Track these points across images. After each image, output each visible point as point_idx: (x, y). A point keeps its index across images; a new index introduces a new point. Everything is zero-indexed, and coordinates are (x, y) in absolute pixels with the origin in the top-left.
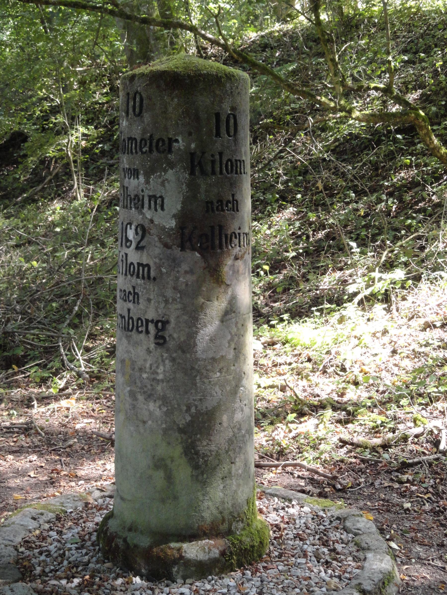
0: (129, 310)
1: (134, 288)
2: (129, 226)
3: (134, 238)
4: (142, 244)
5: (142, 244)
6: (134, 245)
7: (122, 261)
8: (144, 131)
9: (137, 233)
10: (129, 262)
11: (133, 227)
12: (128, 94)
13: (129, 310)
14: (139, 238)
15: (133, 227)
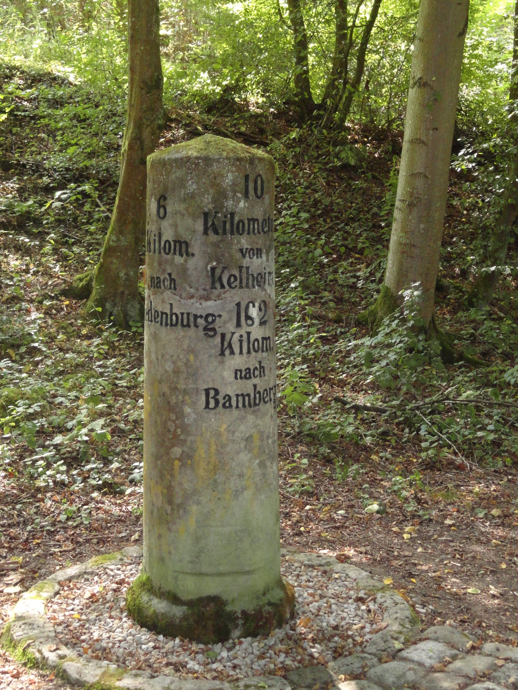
0: (255, 386)
1: (260, 363)
2: (251, 305)
3: (258, 315)
4: (265, 318)
5: (265, 318)
6: (257, 321)
7: (241, 341)
8: (265, 212)
9: (260, 309)
10: (252, 339)
11: (257, 305)
12: (247, 177)
13: (255, 386)
14: (263, 313)
15: (257, 305)
